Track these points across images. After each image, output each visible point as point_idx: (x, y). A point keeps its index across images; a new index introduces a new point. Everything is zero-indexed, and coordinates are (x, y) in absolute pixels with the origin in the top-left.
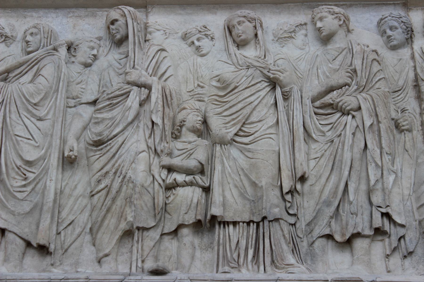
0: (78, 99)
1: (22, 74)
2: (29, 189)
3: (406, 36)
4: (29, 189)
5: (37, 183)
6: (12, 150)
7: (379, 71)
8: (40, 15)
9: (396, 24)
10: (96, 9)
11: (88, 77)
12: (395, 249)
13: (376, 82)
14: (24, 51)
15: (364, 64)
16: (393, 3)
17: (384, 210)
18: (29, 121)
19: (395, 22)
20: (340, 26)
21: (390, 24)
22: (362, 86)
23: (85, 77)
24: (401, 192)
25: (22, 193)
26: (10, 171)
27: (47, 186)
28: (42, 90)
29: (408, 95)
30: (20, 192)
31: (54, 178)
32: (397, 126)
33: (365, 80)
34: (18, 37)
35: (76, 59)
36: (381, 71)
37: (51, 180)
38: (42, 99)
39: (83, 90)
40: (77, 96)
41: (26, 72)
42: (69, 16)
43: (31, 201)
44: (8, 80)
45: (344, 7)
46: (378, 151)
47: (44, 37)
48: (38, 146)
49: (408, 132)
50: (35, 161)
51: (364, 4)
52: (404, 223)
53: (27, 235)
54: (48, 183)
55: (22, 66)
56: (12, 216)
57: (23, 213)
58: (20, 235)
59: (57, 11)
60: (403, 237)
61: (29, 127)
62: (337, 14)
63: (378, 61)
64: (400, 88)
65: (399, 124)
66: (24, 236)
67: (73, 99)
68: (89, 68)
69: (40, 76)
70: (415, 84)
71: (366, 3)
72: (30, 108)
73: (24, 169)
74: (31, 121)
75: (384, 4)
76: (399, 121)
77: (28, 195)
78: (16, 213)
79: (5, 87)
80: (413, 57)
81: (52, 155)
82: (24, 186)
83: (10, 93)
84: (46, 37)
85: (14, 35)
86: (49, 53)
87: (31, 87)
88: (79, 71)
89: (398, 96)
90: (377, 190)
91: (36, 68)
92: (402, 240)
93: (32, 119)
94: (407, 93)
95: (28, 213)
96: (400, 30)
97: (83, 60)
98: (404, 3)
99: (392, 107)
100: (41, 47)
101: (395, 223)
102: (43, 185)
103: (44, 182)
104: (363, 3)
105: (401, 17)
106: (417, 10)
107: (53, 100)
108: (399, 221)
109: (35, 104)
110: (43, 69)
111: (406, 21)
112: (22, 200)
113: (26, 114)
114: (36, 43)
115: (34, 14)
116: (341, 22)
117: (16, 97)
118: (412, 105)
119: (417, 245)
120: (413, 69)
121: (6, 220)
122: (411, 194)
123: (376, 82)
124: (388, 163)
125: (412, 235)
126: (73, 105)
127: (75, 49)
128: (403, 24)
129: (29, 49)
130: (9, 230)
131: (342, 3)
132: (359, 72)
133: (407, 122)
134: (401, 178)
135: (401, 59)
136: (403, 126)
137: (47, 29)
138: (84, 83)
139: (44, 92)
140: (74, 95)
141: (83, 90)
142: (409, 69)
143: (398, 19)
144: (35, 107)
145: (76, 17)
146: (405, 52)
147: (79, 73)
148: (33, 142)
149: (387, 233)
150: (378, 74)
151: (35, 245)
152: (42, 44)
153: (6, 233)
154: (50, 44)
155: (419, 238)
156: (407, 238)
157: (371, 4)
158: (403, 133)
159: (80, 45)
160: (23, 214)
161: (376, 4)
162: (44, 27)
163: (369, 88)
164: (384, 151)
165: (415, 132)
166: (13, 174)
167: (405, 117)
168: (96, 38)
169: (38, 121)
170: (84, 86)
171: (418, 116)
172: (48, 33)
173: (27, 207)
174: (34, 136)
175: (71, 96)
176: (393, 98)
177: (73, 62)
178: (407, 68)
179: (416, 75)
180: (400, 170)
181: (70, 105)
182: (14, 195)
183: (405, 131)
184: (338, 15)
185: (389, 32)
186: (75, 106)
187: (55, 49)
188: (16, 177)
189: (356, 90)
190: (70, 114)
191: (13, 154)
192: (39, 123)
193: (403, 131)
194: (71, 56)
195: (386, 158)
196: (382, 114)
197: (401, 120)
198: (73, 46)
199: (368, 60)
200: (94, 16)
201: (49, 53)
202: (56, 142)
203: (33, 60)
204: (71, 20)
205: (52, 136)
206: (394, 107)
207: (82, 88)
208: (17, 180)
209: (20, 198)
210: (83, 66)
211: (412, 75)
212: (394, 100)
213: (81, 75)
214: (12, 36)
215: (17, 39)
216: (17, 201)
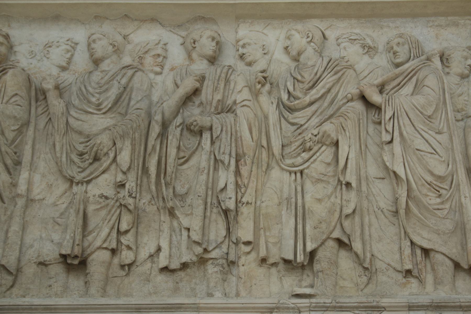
0: (464, 113)
1: (400, 86)
2: (447, 206)
4: (447, 206)
5: (452, 201)
6: (417, 166)
8: (397, 25)
10: (457, 18)
11: (469, 89)
14: (390, 63)
18: (427, 134)
23: (466, 89)
25: (441, 211)
26: (420, 187)
27: (463, 203)
28: (432, 102)
30: (438, 209)
31: (467, 195)
34: (379, 48)
35: (451, 70)
37: (465, 197)
38: (434, 111)
39: (466, 102)
40: (462, 109)
41: (404, 84)
42: (429, 25)
43: (452, 219)
44: (386, 92)
47: (413, 47)
48: (444, 161)
50: (446, 176)
53: (456, 256)
54: (463, 199)
55: (397, 77)
56: (437, 235)
57: (448, 231)
58: (449, 256)
59: (415, 20)
61: (429, 141)
66: (453, 257)
67: (458, 112)
68: (467, 80)
69: (425, 87)
72: (426, 120)
73: (435, 185)
74: (430, 135)
77: (448, 213)
78: (440, 232)
79: (392, 99)
81: (459, 170)
82: (442, 203)
83: (398, 105)
84: (414, 46)
85: (376, 45)
86: (424, 63)
87: (419, 100)
88: (457, 83)
91: (414, 79)
93: (430, 132)
95: (453, 231)
97: (459, 71)
100: (412, 57)
102: (458, 202)
103: (458, 200)
107: (444, 112)
109: (429, 117)
110: (426, 80)
112: (444, 218)
113: (422, 127)
114: (405, 53)
115: (391, 25)
117: (407, 109)
121: (429, 240)
126: (461, 119)
127: (447, 59)
129: (398, 61)
130: (437, 250)
137: (414, 39)
138: (466, 95)
139: (435, 103)
140: (458, 108)
141: (466, 102)
144: (429, 119)
145: (437, 26)
147: (457, 84)
148: (437, 156)
151: (466, 267)
152: (412, 55)
153: (432, 254)
154: (422, 55)
159: (452, 56)
160: (448, 233)
162: (410, 38)
166: (425, 191)
168: (467, 48)
169: (437, 135)
170: (466, 98)
172: (415, 43)
173: (448, 225)
174: (437, 150)
175: (456, 109)
177: (448, 73)
181: (457, 118)
182: (434, 213)
186: (462, 120)
187: (428, 59)
188: (428, 194)
190: (461, 128)
191: (419, 169)
192: (438, 137)
194: (444, 67)
198: (444, 56)
200: (456, 25)
201: (424, 63)
202: (459, 156)
203: (409, 70)
204: (432, 30)
205: (452, 149)
207: (465, 100)
208: (430, 197)
209: (441, 216)
210: (459, 77)
213: (460, 86)
214: (375, 47)
215: (379, 51)
216: (439, 219)
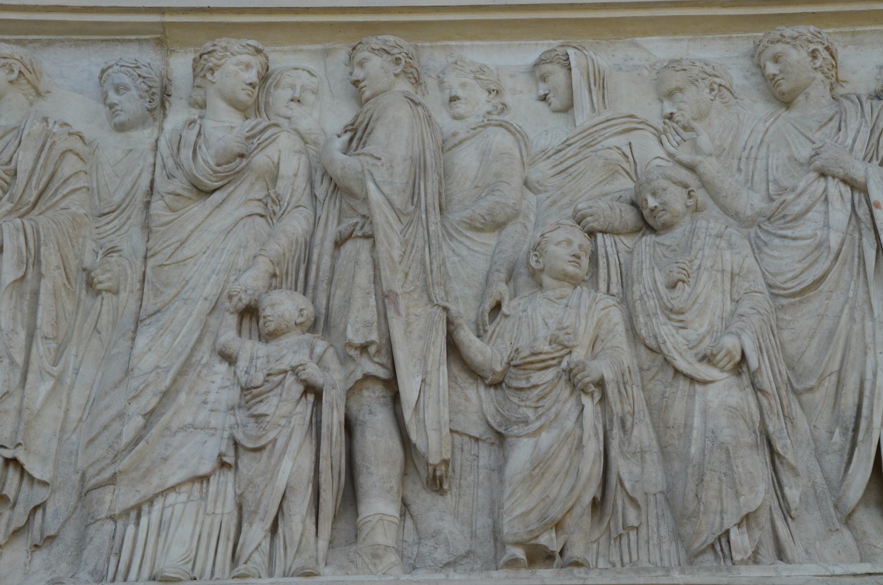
3: (147, 105)
7: (76, 174)
9: (126, 80)
12: (17, 532)
13: (65, 196)
15: (41, 161)
16: (137, 40)
17: (8, 454)
19: (124, 76)
20: (11, 82)
21: (116, 81)
22: (27, 204)
24: (62, 415)
29: (131, 221)
32: (90, 284)
33: (35, 194)
36: (82, 174)
45: (37, 45)
46: (22, 334)
49: (110, 295)
51: (78, 40)
52: (46, 478)
60: (42, 506)
62: (5, 58)
63: (78, 155)
64: (114, 207)
65: (93, 279)
70: (147, 199)
71: (81, 37)
75: (118, 40)
76: (93, 274)
80: (156, 148)
89: (108, 223)
90: (6, 412)
92: (39, 513)
94: (129, 218)
96: (134, 92)
98: (158, 38)
99: (90, 245)
101: (32, 479)
104: (74, 37)
105: (138, 67)
106: (186, 53)
108: (37, 475)
111: (146, 75)
116: (14, 76)
118: (131, 240)
119: (65, 522)
120: (151, 169)
122: (84, 419)
123: (65, 196)
124: (41, 357)
125: (60, 504)
128: (141, 80)
131: (30, 37)
132: (22, 178)
133: (108, 275)
134: (72, 387)
135: (131, 150)
136: (100, 282)
142: (142, 170)
143: (131, 70)
146: (144, 136)
149: (9, 500)
150: (72, 180)
155: (76, 508)
156: (50, 509)
157: (92, 40)
158: (100, 297)
161: (102, 41)
163: (43, 208)
164: (39, 334)
165: (123, 295)
167: (107, 265)
171: (139, 262)
176: (97, 228)
178: (139, 168)
179: (152, 182)
180: (70, 372)
183: (104, 293)
184: (7, 60)
185: (113, 97)
189: (10, 212)
193: (99, 292)
195: (40, 348)
196: (50, 258)
197: (98, 271)
199: (54, 152)
206: (94, 245)
211: (145, 182)
212: (97, 231)
